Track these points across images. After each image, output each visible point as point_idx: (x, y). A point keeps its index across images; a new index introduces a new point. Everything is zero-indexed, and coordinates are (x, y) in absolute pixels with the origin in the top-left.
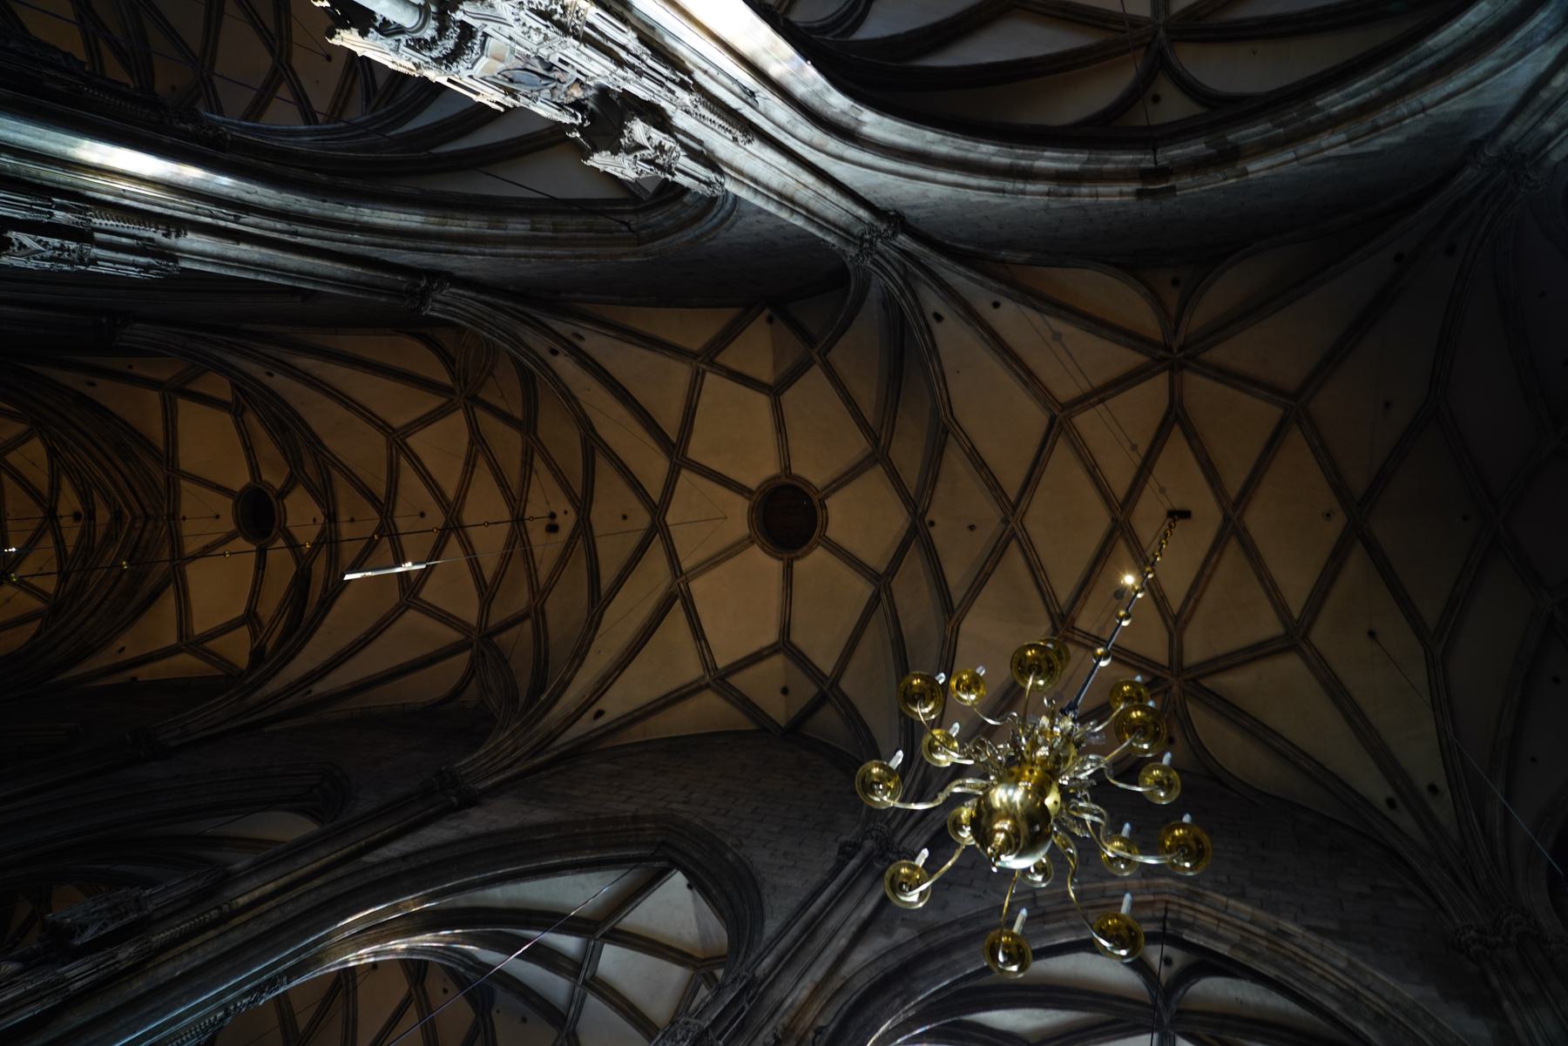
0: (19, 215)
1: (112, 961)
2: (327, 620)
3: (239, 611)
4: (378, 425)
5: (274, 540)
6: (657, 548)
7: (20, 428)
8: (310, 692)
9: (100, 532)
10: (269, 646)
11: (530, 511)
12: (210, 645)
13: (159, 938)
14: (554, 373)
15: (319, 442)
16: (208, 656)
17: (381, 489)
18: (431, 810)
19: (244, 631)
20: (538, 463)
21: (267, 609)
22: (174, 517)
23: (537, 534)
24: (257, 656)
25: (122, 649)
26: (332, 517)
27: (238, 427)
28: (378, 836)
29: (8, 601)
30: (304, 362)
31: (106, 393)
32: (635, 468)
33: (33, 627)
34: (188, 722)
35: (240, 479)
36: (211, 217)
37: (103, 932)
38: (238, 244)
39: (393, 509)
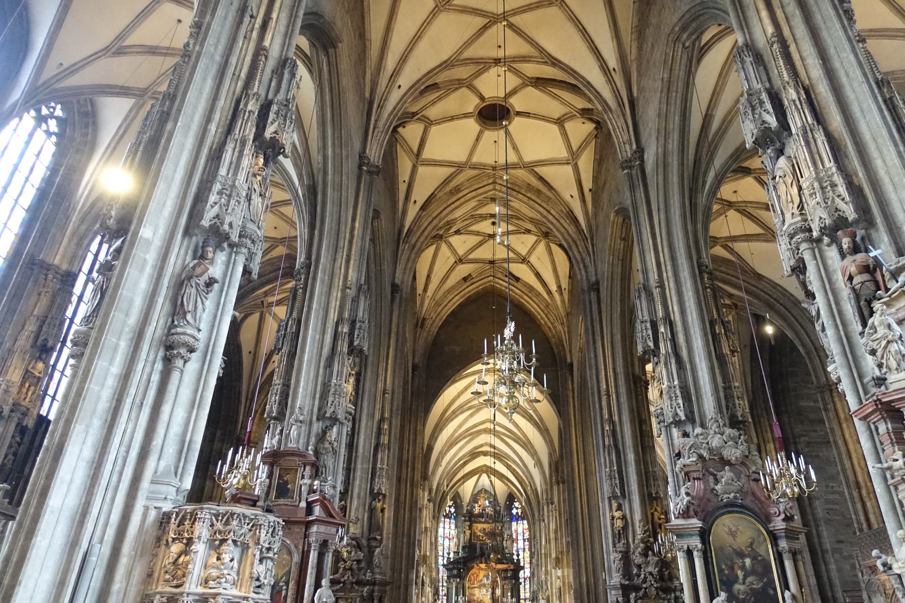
1: (798, 102)
2: (566, 61)
3: (555, 128)
4: (432, 18)
5: (512, 105)
7: (444, 247)
8: (614, 69)
12: (575, 149)
15: (445, 62)
16: (582, 147)
25: (572, 196)
26: (497, 61)
27: (439, 123)
29: (539, 259)
30: (390, 63)
31: (420, 195)
33: (554, 247)
35: (472, 126)
36: (252, 31)
37: (771, 111)
38: (272, 19)
39: (493, 14)
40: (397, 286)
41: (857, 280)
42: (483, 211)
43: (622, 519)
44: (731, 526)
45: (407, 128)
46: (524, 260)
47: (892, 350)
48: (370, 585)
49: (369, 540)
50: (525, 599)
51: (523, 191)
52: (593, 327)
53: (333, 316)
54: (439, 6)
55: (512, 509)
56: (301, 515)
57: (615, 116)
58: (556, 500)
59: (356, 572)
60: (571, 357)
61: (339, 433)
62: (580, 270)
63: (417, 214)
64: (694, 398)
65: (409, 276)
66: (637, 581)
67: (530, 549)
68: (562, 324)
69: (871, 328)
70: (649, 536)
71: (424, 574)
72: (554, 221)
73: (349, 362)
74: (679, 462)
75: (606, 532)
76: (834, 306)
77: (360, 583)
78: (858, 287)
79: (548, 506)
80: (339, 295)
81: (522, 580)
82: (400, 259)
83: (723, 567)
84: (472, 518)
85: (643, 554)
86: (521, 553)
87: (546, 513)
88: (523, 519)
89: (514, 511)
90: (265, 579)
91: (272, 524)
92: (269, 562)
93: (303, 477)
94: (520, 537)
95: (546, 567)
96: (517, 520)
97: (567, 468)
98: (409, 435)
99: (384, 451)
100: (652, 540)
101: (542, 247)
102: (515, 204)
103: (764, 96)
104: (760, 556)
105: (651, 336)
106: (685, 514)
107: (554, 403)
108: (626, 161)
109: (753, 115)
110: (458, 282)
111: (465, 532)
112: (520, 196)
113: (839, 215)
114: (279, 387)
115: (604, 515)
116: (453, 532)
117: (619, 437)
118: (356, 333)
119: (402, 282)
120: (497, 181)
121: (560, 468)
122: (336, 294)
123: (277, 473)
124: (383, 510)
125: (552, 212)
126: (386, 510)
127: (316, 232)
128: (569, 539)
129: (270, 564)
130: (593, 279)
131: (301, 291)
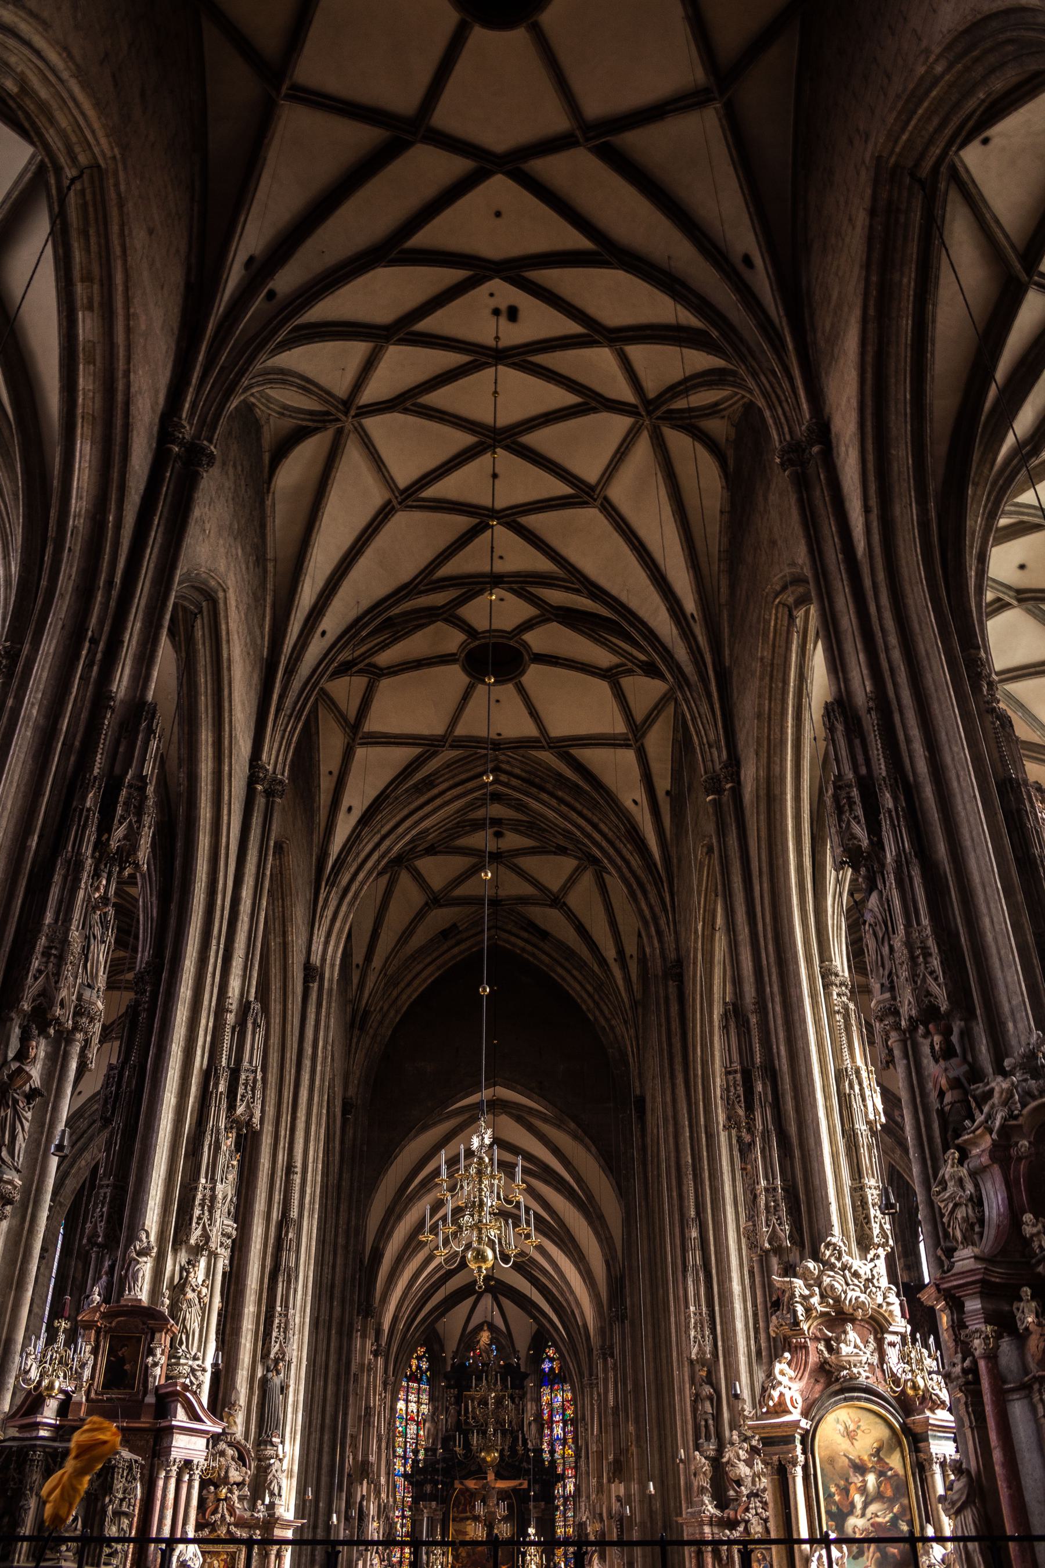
0: (91, 835)
1: (894, 813)
2: (614, 591)
5: (526, 645)
6: (542, 167)
7: (405, 879)
8: (692, 615)
9: (511, 814)
10: (643, 658)
11: (490, 342)
13: (881, 768)
14: (300, 296)
15: (405, 586)
17: (462, 522)
18: (822, 476)
19: (626, 682)
20: (424, 325)
21: (604, 658)
22: (497, 745)
23: (513, 335)
24: (650, 670)
25: (635, 802)
26: (496, 580)
27: (396, 673)
28: (836, 540)
32: (429, 192)
34: (705, 740)
35: (455, 676)
37: (863, 820)
40: (315, 969)
41: (948, 1098)
42: (480, 813)
43: (711, 1399)
44: (849, 1422)
46: (557, 901)
47: (959, 1217)
51: (549, 786)
52: (670, 1045)
53: (200, 1061)
54: (395, 502)
55: (543, 1361)
57: (695, 695)
59: (237, 1505)
60: (642, 1086)
61: (210, 1272)
62: (650, 937)
63: (353, 831)
64: (803, 1208)
65: (337, 946)
67: (575, 1440)
68: (626, 1022)
69: (940, 1183)
71: (363, 1497)
72: (604, 844)
73: (228, 1143)
74: (774, 1317)
75: (684, 1422)
76: (923, 1130)
78: (947, 1108)
80: (211, 1025)
81: (559, 1502)
82: (321, 917)
83: (833, 1490)
85: (744, 1461)
86: (559, 1448)
87: (601, 1375)
88: (563, 1381)
89: (546, 1366)
93: (151, 1352)
94: (557, 1418)
95: (600, 1477)
96: (551, 1383)
98: (336, 1236)
101: (587, 879)
103: (855, 793)
104: (891, 1469)
105: (742, 1099)
107: (611, 1170)
108: (712, 779)
109: (840, 820)
110: (432, 940)
111: (447, 1409)
112: (544, 796)
113: (930, 1001)
114: (109, 1190)
115: (681, 1391)
116: (425, 1409)
117: (712, 1248)
118: (241, 1090)
119: (323, 959)
120: (504, 766)
122: (206, 1022)
123: (105, 1345)
124: (284, 1389)
125: (602, 826)
126: (291, 1389)
127: (173, 907)
130: (673, 956)
131: (144, 1015)
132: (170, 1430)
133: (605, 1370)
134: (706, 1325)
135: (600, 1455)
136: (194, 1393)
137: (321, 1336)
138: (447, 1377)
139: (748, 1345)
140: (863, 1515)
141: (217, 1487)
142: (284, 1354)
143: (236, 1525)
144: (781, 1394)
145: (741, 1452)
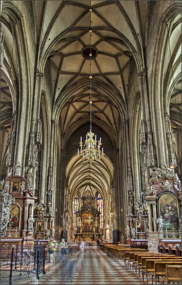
9: (93, 92)
43: (132, 197)
45: (54, 58)
48: (48, 218)
49: (47, 204)
50: (102, 222)
51: (101, 85)
56: (22, 197)
58: (112, 193)
66: (135, 215)
67: (103, 208)
70: (141, 202)
74: (151, 179)
77: (44, 217)
79: (109, 195)
81: (101, 217)
84: (84, 199)
86: (100, 209)
88: (101, 199)
89: (98, 197)
90: (7, 212)
91: (7, 196)
92: (8, 207)
94: (100, 204)
97: (116, 182)
99: (51, 177)
100: (142, 203)
102: (99, 90)
106: (152, 194)
112: (100, 87)
115: (126, 196)
116: (77, 203)
121: (113, 183)
124: (51, 196)
126: (53, 196)
128: (115, 204)
129: (8, 208)
132: (27, 198)
133: (109, 196)
134: (131, 185)
135: (108, 209)
136: (31, 192)
137: (58, 189)
138: (81, 198)
139: (140, 188)
140: (168, 214)
141: (40, 211)
142: (51, 189)
143: (44, 217)
144: (152, 192)
145: (138, 206)
